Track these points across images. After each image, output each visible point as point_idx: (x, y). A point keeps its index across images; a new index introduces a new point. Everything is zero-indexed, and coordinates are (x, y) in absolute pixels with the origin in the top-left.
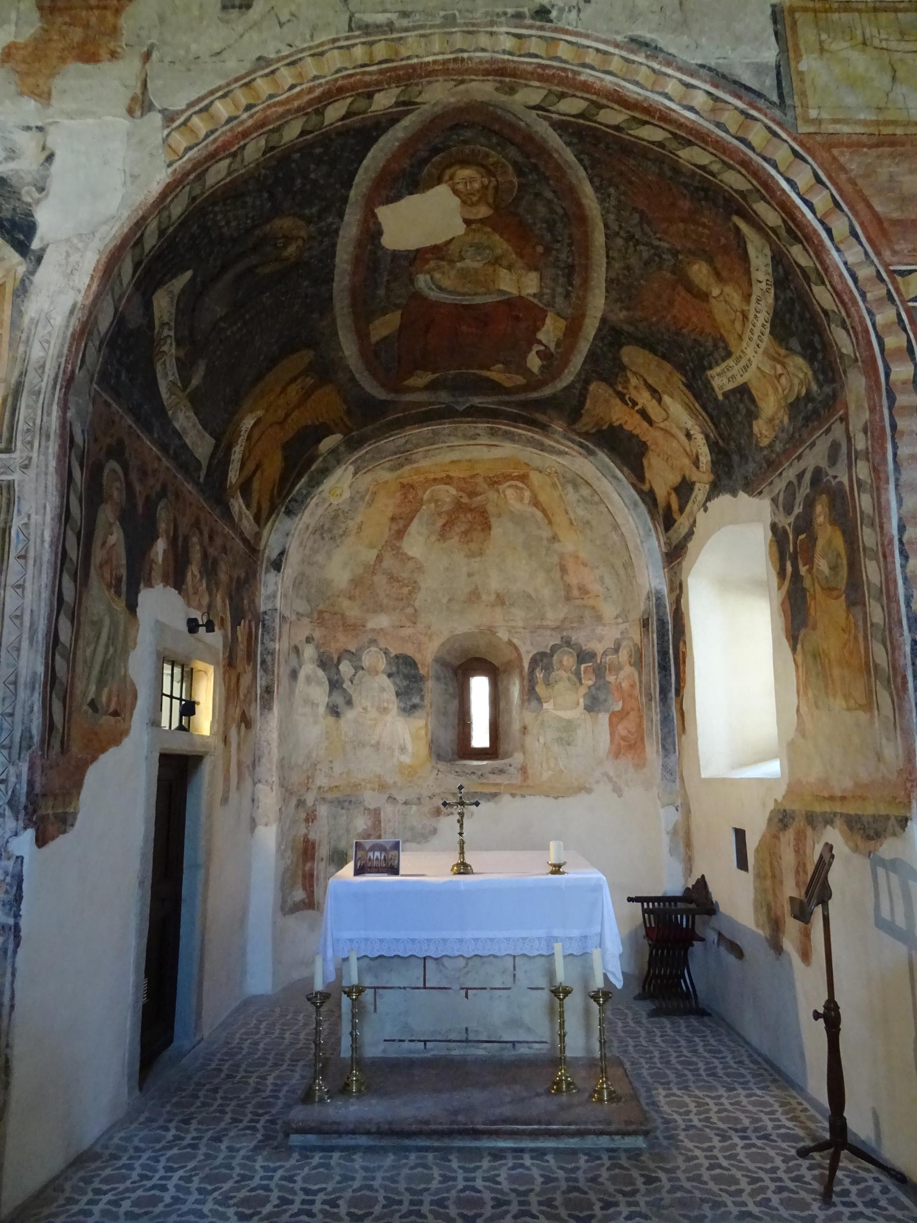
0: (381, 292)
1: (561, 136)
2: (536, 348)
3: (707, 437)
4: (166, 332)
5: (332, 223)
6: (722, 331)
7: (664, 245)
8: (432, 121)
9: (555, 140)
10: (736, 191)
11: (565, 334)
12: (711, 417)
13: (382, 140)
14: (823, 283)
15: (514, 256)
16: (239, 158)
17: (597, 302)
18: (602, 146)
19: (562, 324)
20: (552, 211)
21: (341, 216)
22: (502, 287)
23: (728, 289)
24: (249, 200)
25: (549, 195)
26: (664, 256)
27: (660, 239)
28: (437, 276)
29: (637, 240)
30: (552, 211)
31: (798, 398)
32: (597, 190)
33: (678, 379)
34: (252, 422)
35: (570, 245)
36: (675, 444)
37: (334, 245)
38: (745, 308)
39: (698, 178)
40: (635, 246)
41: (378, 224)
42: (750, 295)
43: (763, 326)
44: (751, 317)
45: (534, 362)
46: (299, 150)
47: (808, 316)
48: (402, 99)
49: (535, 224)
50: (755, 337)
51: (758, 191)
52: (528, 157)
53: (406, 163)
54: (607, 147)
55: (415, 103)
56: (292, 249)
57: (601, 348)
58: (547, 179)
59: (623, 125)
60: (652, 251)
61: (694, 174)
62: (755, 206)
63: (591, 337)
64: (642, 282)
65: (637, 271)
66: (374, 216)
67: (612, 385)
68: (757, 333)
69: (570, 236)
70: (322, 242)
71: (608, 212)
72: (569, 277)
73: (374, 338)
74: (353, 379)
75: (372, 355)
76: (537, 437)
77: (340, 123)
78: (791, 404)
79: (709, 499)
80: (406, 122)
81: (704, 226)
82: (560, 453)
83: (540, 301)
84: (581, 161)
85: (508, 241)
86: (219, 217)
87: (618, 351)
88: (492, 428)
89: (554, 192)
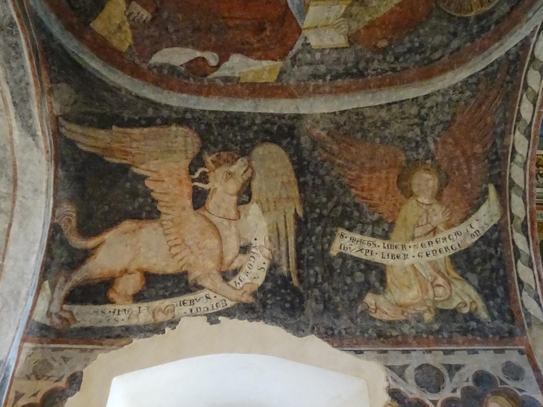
1: (516, 46)
2: (212, 58)
3: (273, 266)
6: (399, 223)
7: (432, 147)
9: (511, 42)
10: (510, 178)
11: (253, 84)
12: (299, 257)
14: (531, 267)
15: (368, 19)
17: (318, 107)
18: (508, 78)
19: (271, 78)
20: (435, 49)
22: (311, 9)
23: (437, 207)
25: (455, 44)
26: (420, 150)
27: (435, 142)
29: (422, 124)
30: (435, 49)
31: (455, 312)
32: (465, 82)
33: (294, 207)
35: (393, 70)
36: (212, 242)
38: (441, 227)
39: (505, 151)
40: (416, 124)
42: (453, 226)
43: (446, 248)
44: (440, 236)
45: (178, 56)
47: (501, 272)
49: (418, 37)
50: (431, 248)
51: (524, 192)
52: (497, 22)
54: (508, 82)
57: (254, 124)
58: (472, 40)
59: (529, 90)
60: (418, 139)
61: (507, 147)
62: (514, 196)
63: (264, 111)
64: (378, 140)
65: (387, 132)
67: (203, 148)
68: (435, 246)
69: (404, 69)
71: (443, 95)
72: (347, 74)
76: (33, 90)
78: (442, 311)
79: (229, 313)
81: (469, 169)
82: (29, 129)
83: (299, 51)
84: (492, 64)
85: (392, 12)
87: (264, 141)
88: (12, 24)
89: (458, 49)
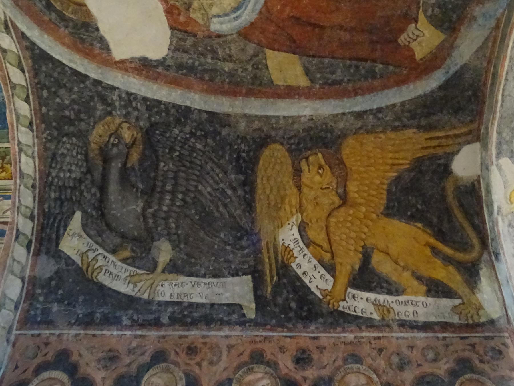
0: (227, 67)
4: (91, 255)
5: (120, 97)
8: (21, 8)
13: (43, 46)
16: (25, 148)
21: (113, 88)
24: (62, 150)
28: (215, 10)
34: (295, 231)
37: (145, 99)
41: (132, 60)
46: (40, 105)
48: (3, 30)
53: (63, 31)
55: (6, 21)
56: (127, 135)
66: (122, 62)
70: (136, 109)
73: (303, 82)
74: (359, 115)
75: (327, 87)
77: (27, 74)
80: (23, 27)
86: (62, 175)
